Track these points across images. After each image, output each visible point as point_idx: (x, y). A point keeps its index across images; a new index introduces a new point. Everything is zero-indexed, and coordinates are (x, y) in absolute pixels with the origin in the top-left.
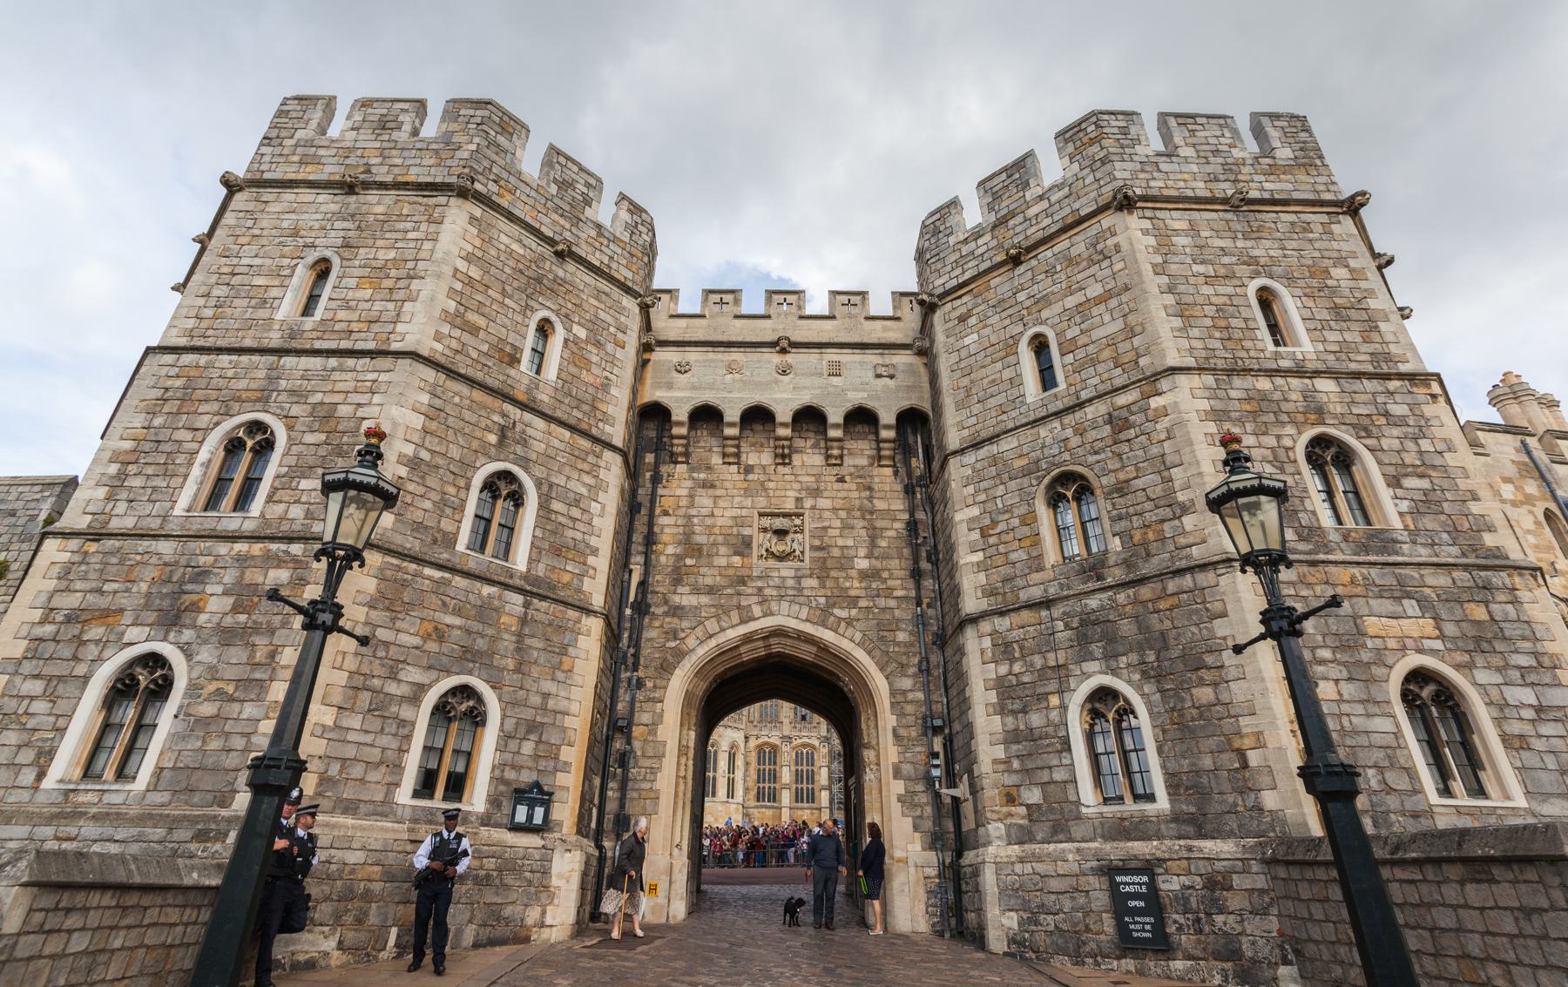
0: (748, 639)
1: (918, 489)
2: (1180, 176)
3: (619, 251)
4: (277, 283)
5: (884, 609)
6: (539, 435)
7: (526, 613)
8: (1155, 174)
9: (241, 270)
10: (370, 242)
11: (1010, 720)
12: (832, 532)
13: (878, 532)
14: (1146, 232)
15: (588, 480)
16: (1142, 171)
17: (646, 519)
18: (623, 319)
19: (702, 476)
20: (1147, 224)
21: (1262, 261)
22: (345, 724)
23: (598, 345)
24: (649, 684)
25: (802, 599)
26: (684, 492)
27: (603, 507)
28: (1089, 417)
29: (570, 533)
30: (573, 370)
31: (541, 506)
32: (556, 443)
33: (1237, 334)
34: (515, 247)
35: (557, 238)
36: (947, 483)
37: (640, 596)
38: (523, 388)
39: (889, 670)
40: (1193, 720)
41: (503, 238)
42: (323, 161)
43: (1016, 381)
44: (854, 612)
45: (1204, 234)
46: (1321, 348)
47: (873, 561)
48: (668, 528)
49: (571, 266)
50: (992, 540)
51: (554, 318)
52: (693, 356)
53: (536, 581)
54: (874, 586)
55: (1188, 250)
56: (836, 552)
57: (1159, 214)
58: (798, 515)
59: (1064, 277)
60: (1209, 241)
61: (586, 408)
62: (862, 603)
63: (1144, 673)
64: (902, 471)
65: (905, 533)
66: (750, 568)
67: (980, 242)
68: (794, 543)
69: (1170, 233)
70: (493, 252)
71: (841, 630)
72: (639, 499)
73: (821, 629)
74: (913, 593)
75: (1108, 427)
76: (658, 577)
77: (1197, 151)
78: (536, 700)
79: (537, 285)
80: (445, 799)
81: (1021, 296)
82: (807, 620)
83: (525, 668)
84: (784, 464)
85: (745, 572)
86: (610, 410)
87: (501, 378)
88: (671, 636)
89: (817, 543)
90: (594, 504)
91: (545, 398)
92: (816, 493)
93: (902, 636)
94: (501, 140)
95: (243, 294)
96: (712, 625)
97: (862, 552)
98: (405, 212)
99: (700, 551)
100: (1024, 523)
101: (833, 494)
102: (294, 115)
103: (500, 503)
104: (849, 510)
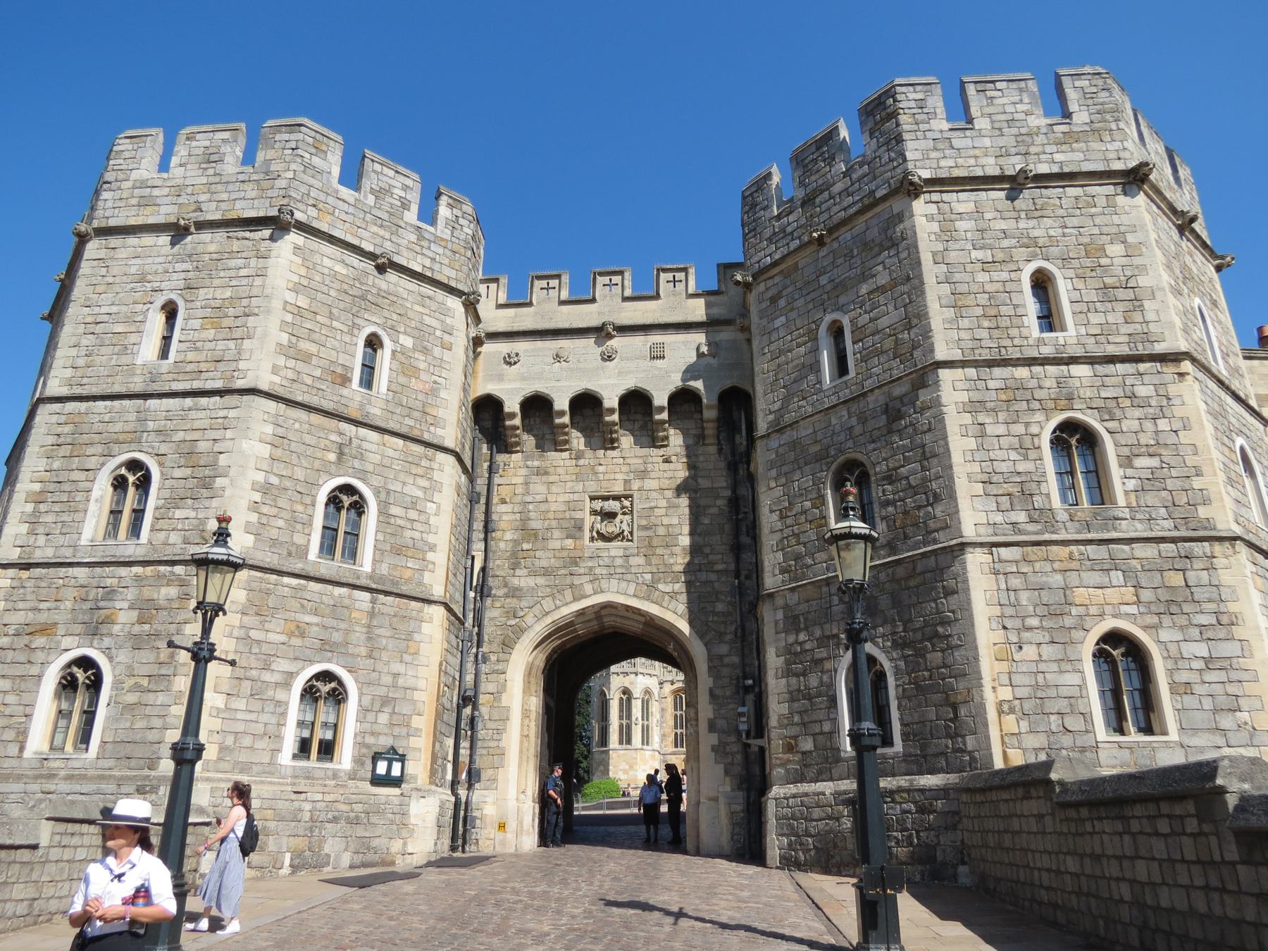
0: (581, 613)
2: (972, 152)
3: (441, 251)
4: (134, 330)
5: (706, 583)
6: (374, 448)
7: (373, 607)
8: (947, 152)
9: (106, 318)
10: (207, 282)
11: (794, 680)
12: (658, 512)
14: (930, 218)
15: (423, 483)
16: (935, 149)
17: (483, 508)
18: (448, 320)
19: (536, 463)
20: (933, 209)
21: (1041, 242)
22: (233, 706)
23: (425, 351)
24: (493, 658)
25: (629, 577)
26: (520, 480)
27: (439, 508)
28: (871, 406)
29: (408, 534)
30: (402, 380)
31: (380, 512)
32: (390, 453)
33: (1004, 322)
34: (339, 268)
35: (378, 252)
38: (356, 405)
39: (708, 637)
40: (925, 680)
41: (327, 262)
42: (158, 201)
43: (815, 367)
45: (988, 216)
46: (1083, 331)
48: (504, 514)
49: (392, 276)
50: (789, 521)
51: (380, 332)
52: (521, 346)
53: (382, 579)
55: (969, 235)
56: (661, 531)
57: (946, 197)
58: (626, 497)
59: (859, 262)
60: (992, 223)
61: (416, 414)
63: (894, 642)
64: (726, 448)
65: (726, 509)
67: (791, 218)
68: (622, 523)
69: (954, 217)
70: (318, 278)
72: (478, 489)
73: (646, 603)
74: (732, 567)
75: (884, 417)
76: (498, 562)
77: (992, 122)
78: (387, 680)
79: (363, 301)
80: (319, 759)
81: (824, 280)
82: (635, 596)
83: (375, 654)
84: (614, 448)
85: (578, 554)
86: (440, 413)
87: (336, 398)
89: (644, 522)
90: (429, 504)
91: (377, 411)
92: (643, 474)
93: (720, 607)
94: (316, 161)
95: (107, 342)
96: (548, 604)
98: (235, 249)
99: (536, 536)
100: (814, 506)
102: (127, 155)
103: (344, 512)
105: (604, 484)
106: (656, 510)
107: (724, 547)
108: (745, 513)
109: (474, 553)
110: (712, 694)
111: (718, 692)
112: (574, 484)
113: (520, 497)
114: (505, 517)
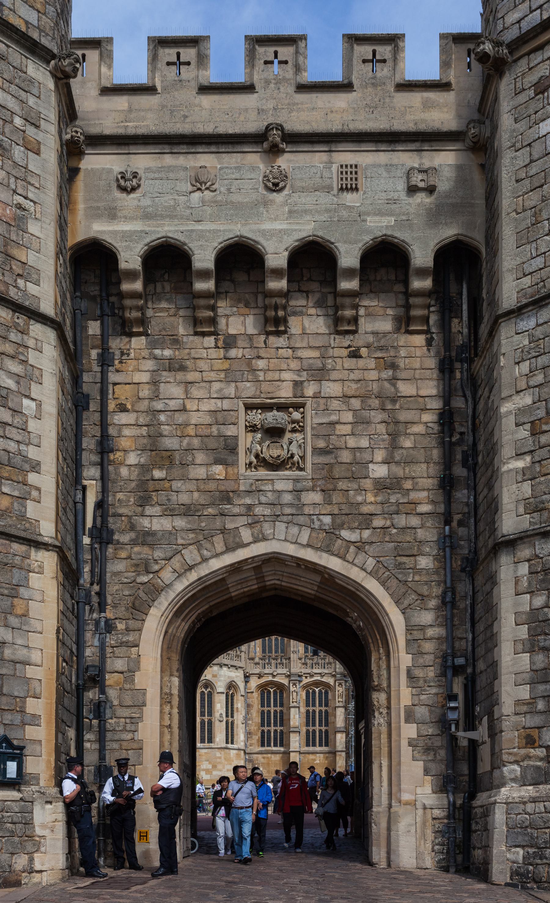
1: (458, 365)
13: (401, 427)
17: (97, 416)
19: (167, 353)
24: (121, 626)
25: (301, 519)
26: (144, 377)
36: (495, 358)
37: (99, 520)
39: (406, 603)
44: (366, 534)
47: (393, 467)
54: (393, 499)
56: (345, 456)
58: (298, 407)
62: (378, 522)
65: (436, 428)
66: (237, 480)
71: (350, 557)
72: (86, 388)
73: (325, 555)
74: (441, 508)
76: (120, 496)
82: (308, 545)
84: (278, 333)
85: (230, 486)
88: (142, 568)
89: (321, 444)
97: (379, 456)
101: (344, 375)
104: (364, 398)
105: (265, 387)
106: (338, 427)
107: (430, 481)
108: (462, 434)
109: (85, 482)
110: (410, 676)
111: (418, 673)
112: (222, 385)
113: (146, 402)
114: (126, 432)
